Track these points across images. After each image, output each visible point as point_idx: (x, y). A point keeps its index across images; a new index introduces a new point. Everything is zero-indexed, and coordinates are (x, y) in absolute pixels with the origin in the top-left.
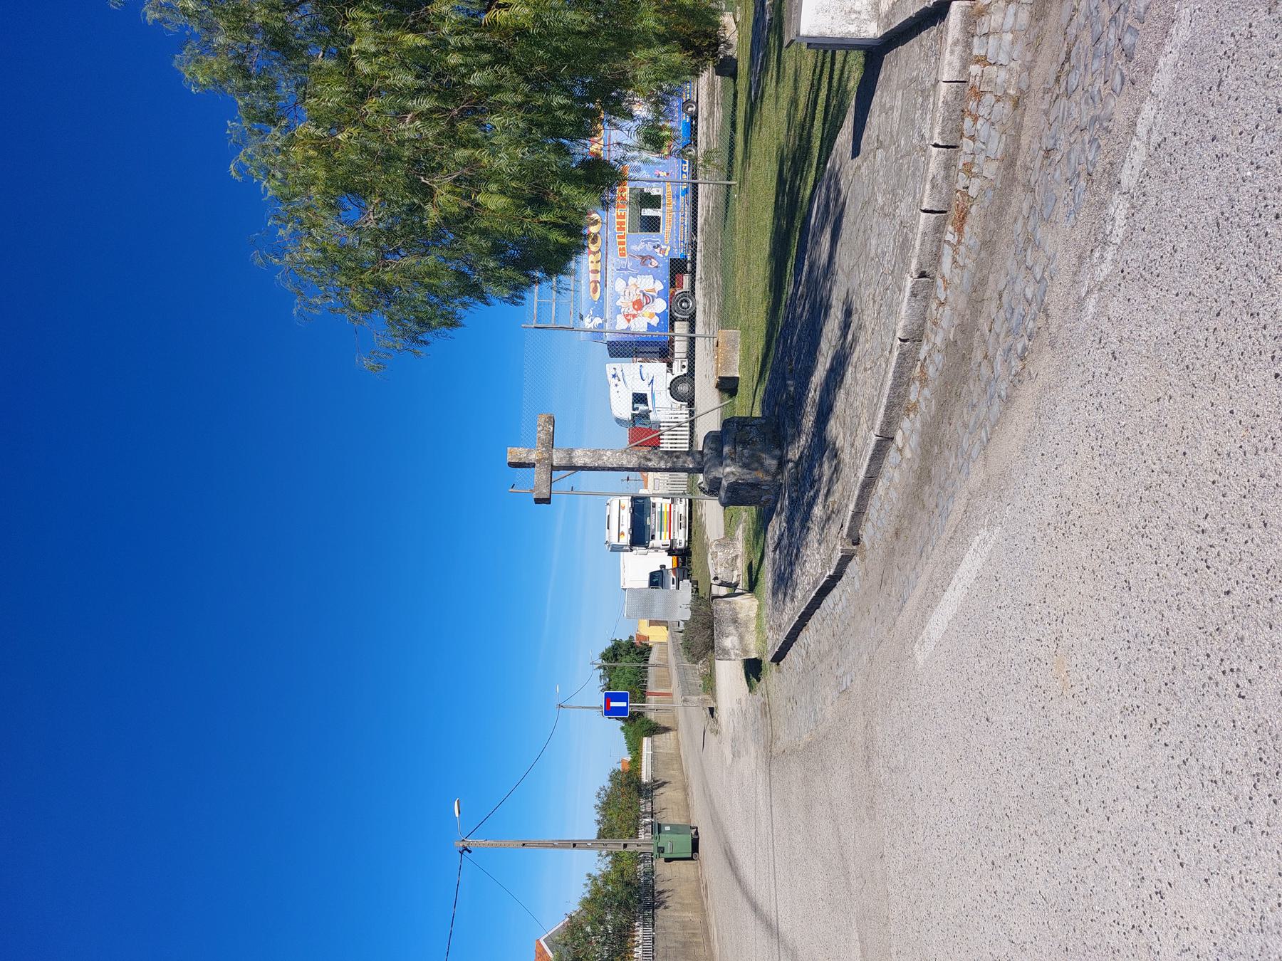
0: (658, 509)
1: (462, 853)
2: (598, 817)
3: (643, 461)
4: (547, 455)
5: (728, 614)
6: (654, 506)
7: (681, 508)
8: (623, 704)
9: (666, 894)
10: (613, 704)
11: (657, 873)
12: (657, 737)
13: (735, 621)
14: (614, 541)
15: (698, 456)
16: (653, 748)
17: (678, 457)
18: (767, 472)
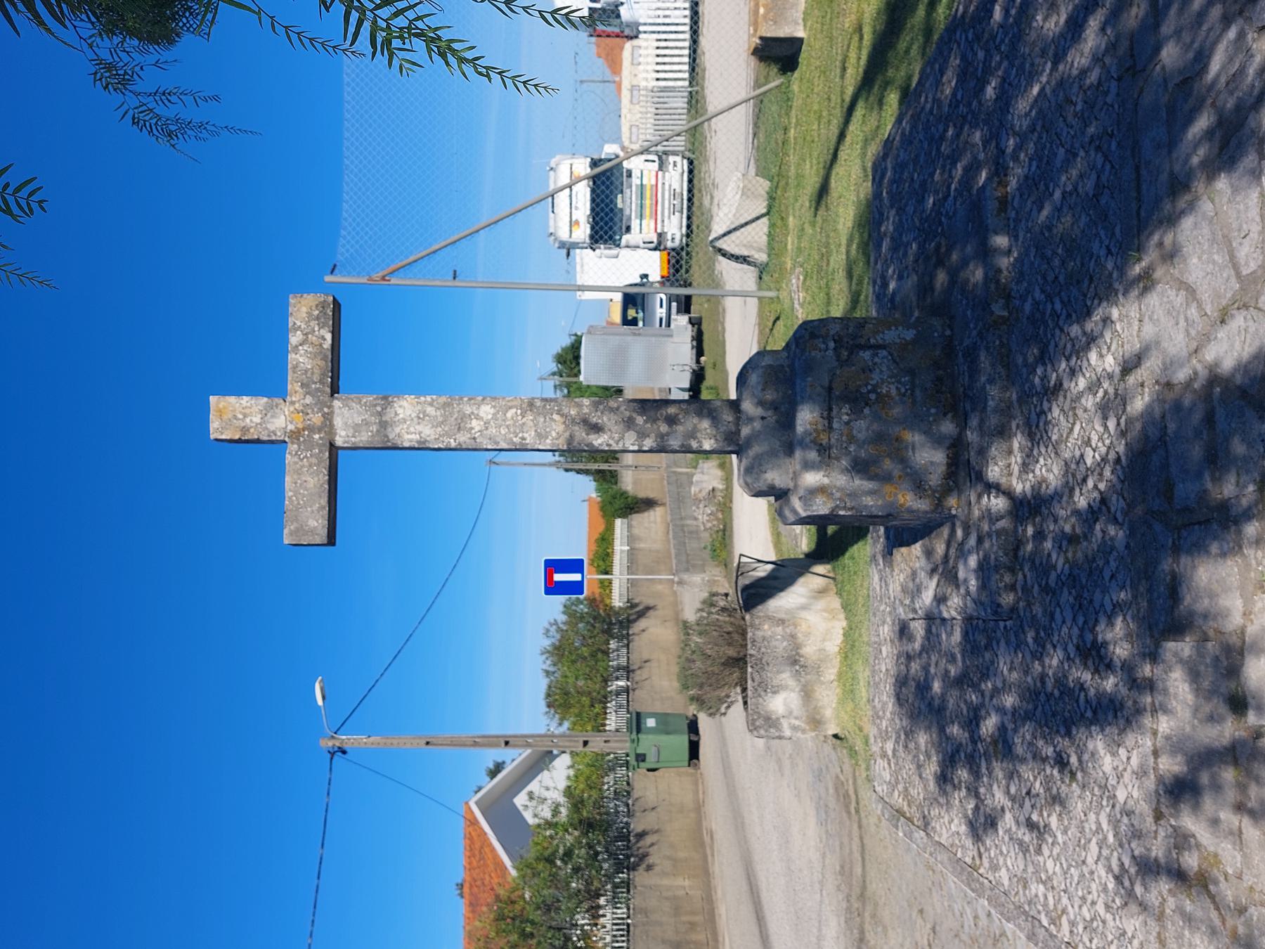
0: (635, 181)
1: (333, 754)
2: (548, 665)
3: (580, 433)
4: (317, 419)
5: (781, 646)
6: (629, 174)
7: (675, 177)
8: (576, 577)
9: (649, 840)
10: (558, 577)
11: (635, 794)
12: (636, 518)
13: (794, 660)
14: (564, 234)
15: (728, 417)
16: (631, 539)
17: (672, 421)
18: (919, 486)
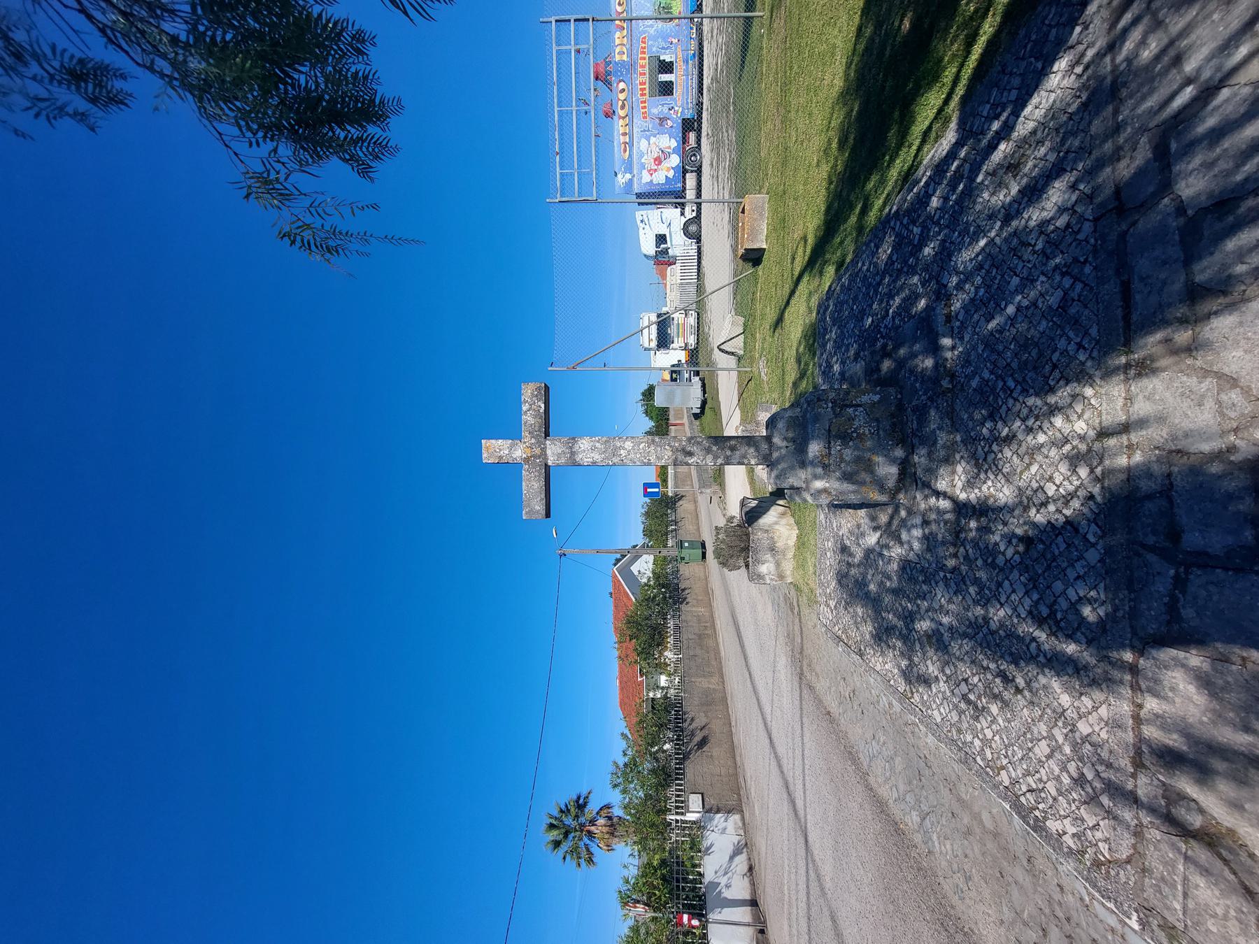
4: (538, 451)
5: (766, 543)
7: (692, 320)
13: (772, 549)
14: (646, 345)
15: (764, 446)
17: (733, 449)
18: (882, 488)
